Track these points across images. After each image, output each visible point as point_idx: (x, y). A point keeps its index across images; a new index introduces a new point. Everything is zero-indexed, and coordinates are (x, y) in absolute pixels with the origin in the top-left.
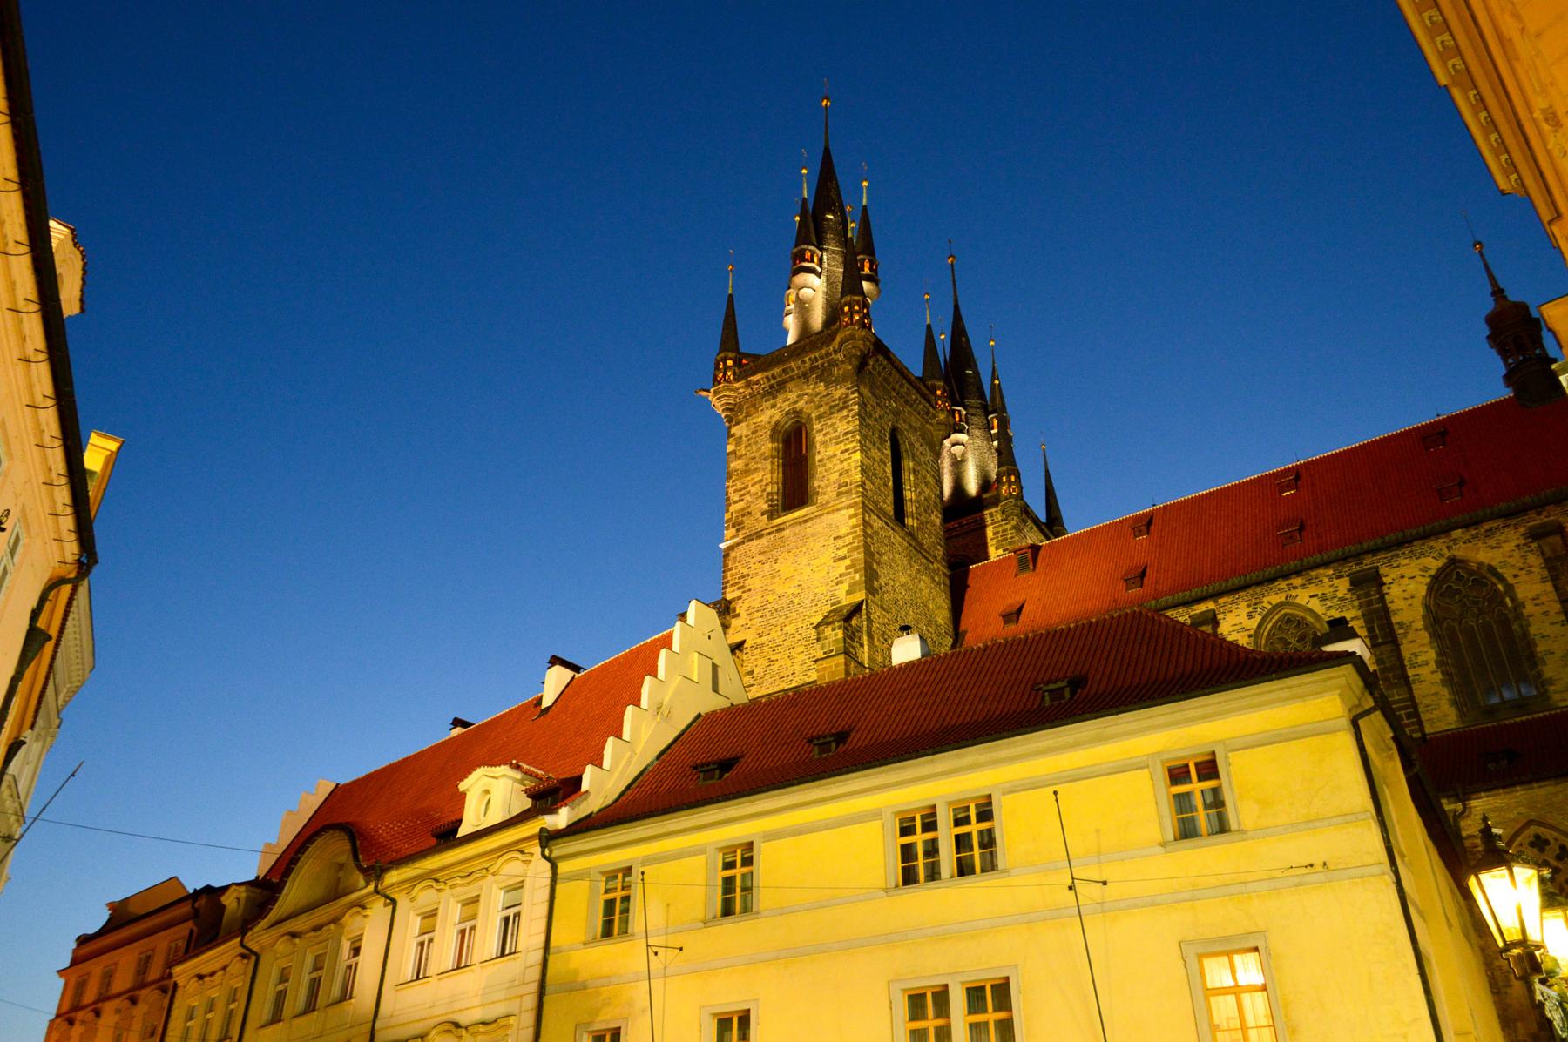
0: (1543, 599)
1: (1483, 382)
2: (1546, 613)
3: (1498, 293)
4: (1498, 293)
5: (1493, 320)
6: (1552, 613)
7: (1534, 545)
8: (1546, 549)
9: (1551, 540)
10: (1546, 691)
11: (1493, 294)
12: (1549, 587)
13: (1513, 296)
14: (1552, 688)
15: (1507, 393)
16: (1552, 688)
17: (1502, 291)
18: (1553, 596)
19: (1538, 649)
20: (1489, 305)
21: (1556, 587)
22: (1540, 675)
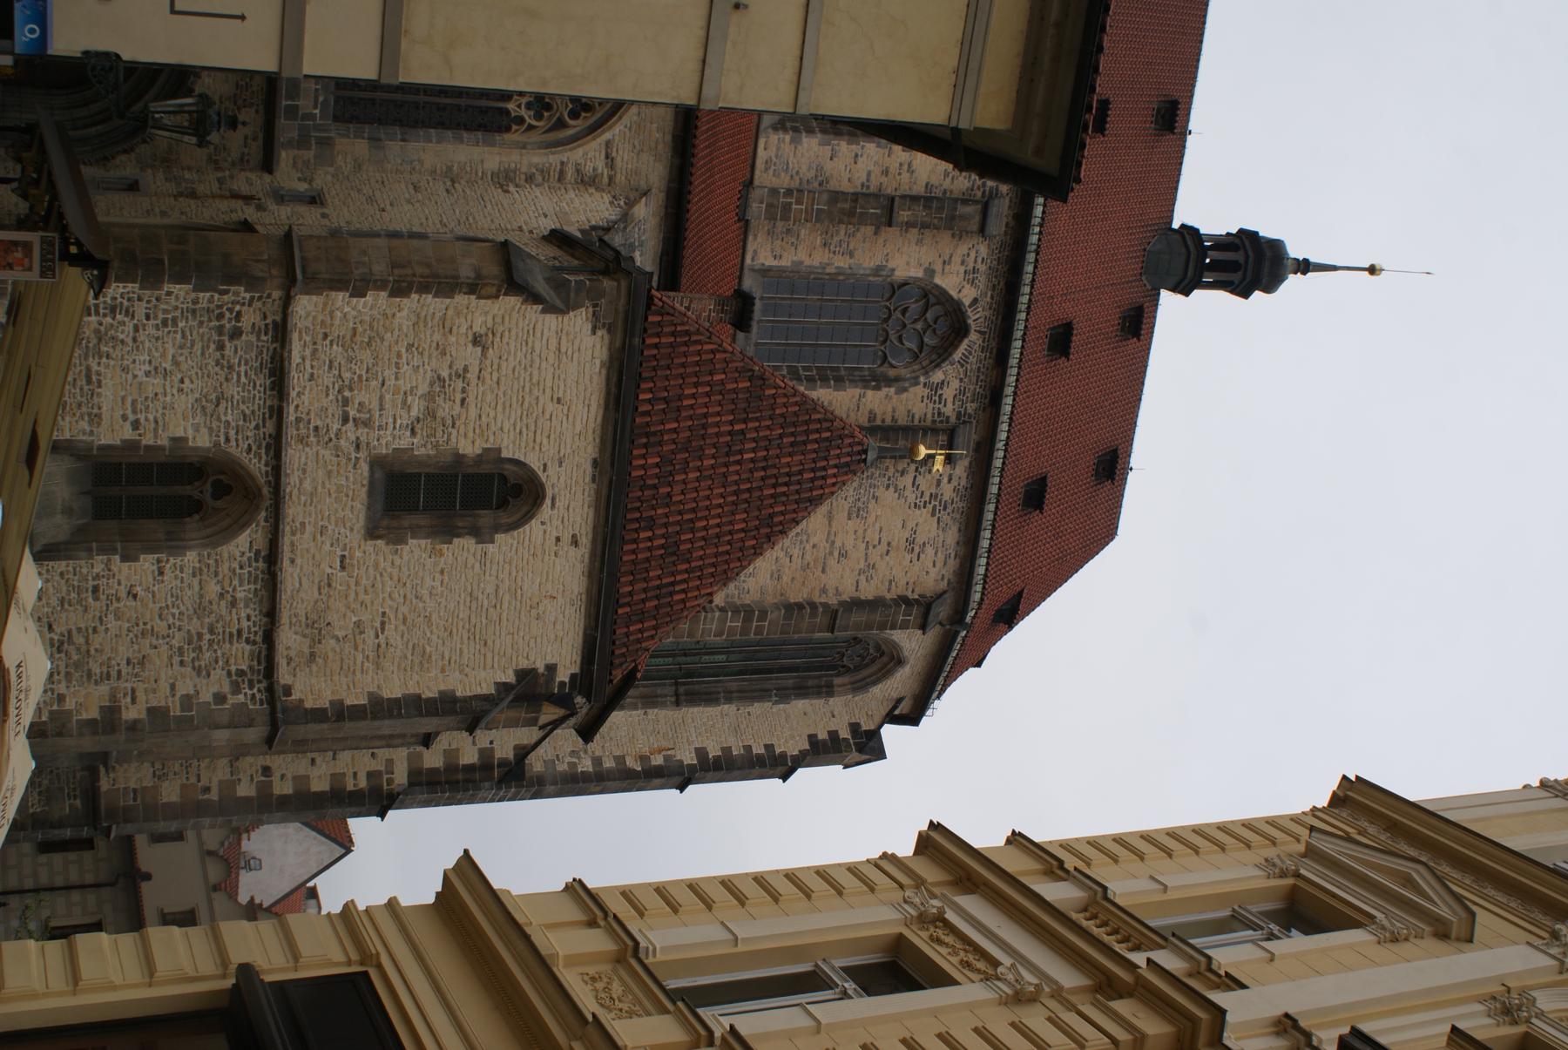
0: (905, 176)
1: (1206, 202)
2: (886, 172)
3: (1305, 267)
4: (1305, 267)
5: (1275, 249)
6: (884, 179)
7: (979, 194)
8: (969, 209)
9: (977, 219)
10: (785, 130)
11: (1306, 261)
12: (919, 189)
13: (1293, 283)
14: (787, 138)
15: (1176, 225)
16: (787, 138)
17: (1304, 273)
18: (905, 189)
19: (843, 144)
20: (1295, 251)
21: (915, 199)
22: (810, 131)
